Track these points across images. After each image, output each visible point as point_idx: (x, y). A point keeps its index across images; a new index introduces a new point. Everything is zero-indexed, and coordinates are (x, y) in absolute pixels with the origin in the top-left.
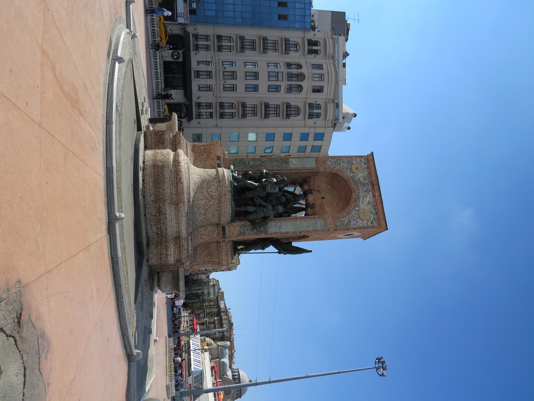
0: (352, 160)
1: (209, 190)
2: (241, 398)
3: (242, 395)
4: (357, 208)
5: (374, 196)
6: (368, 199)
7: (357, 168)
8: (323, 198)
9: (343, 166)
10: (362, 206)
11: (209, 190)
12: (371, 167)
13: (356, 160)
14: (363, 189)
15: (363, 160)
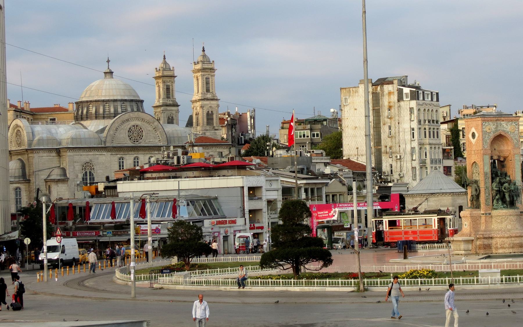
0: (484, 131)
1: (514, 221)
2: (142, 101)
3: (138, 96)
4: (509, 133)
5: (503, 120)
6: (505, 125)
7: (489, 129)
8: (495, 149)
9: (487, 138)
10: (508, 130)
11: (514, 221)
12: (488, 119)
13: (484, 128)
14: (500, 127)
15: (484, 124)
